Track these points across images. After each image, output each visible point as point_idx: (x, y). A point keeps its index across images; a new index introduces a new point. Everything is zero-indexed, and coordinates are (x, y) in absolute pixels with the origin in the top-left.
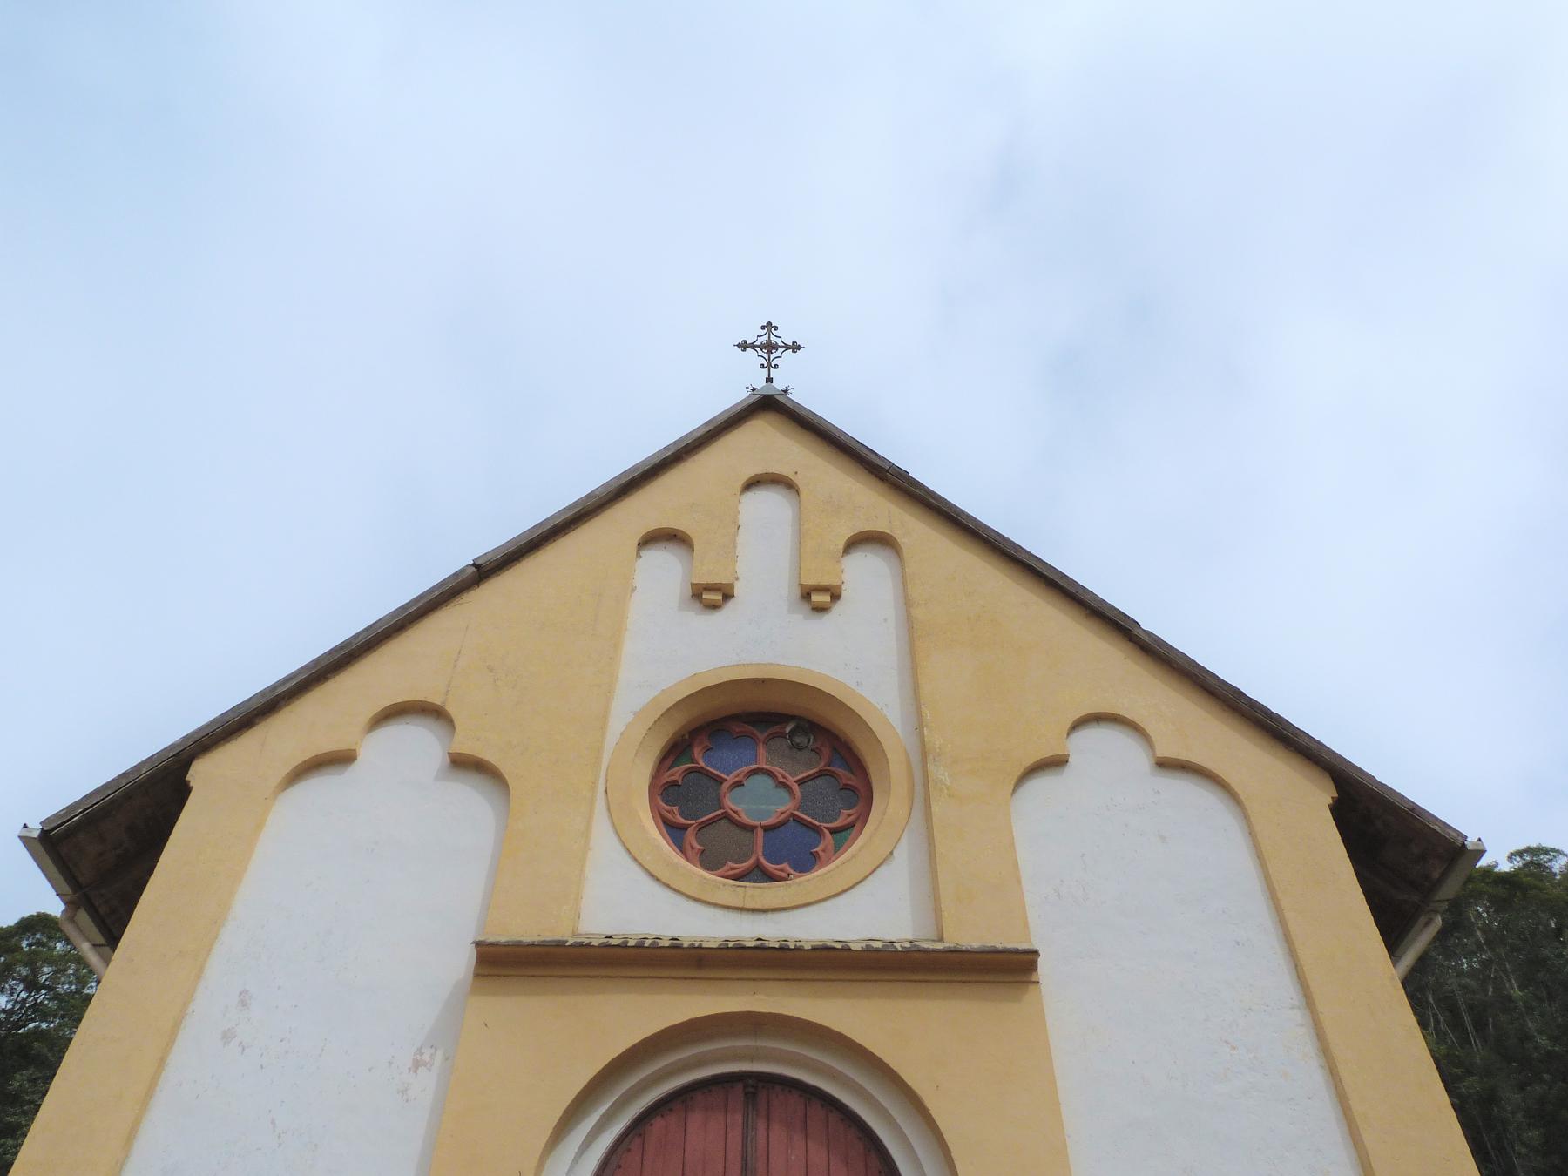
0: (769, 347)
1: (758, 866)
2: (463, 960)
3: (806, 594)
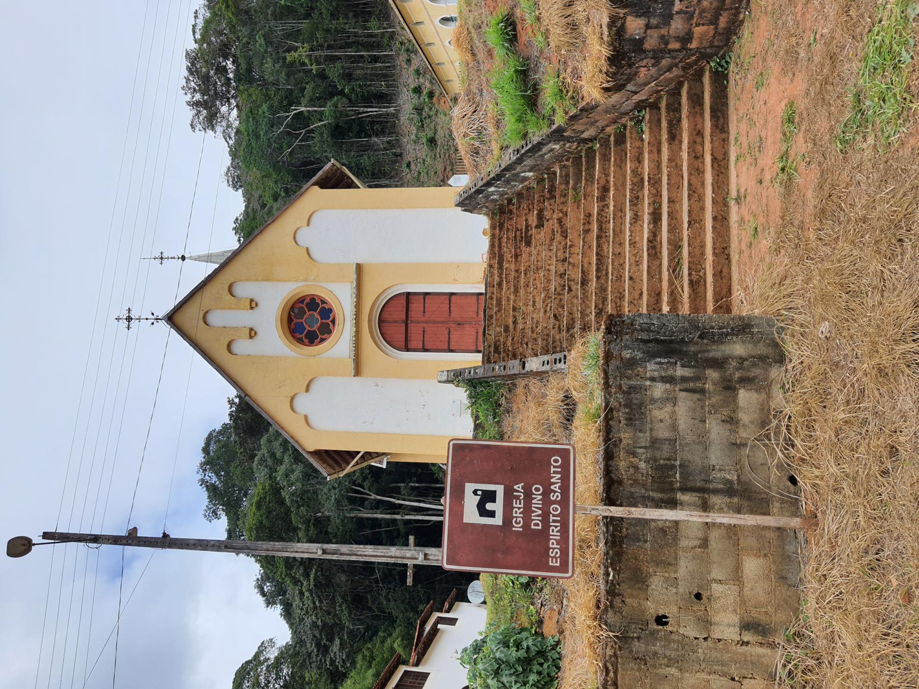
0: (129, 319)
1: (331, 321)
3: (252, 308)
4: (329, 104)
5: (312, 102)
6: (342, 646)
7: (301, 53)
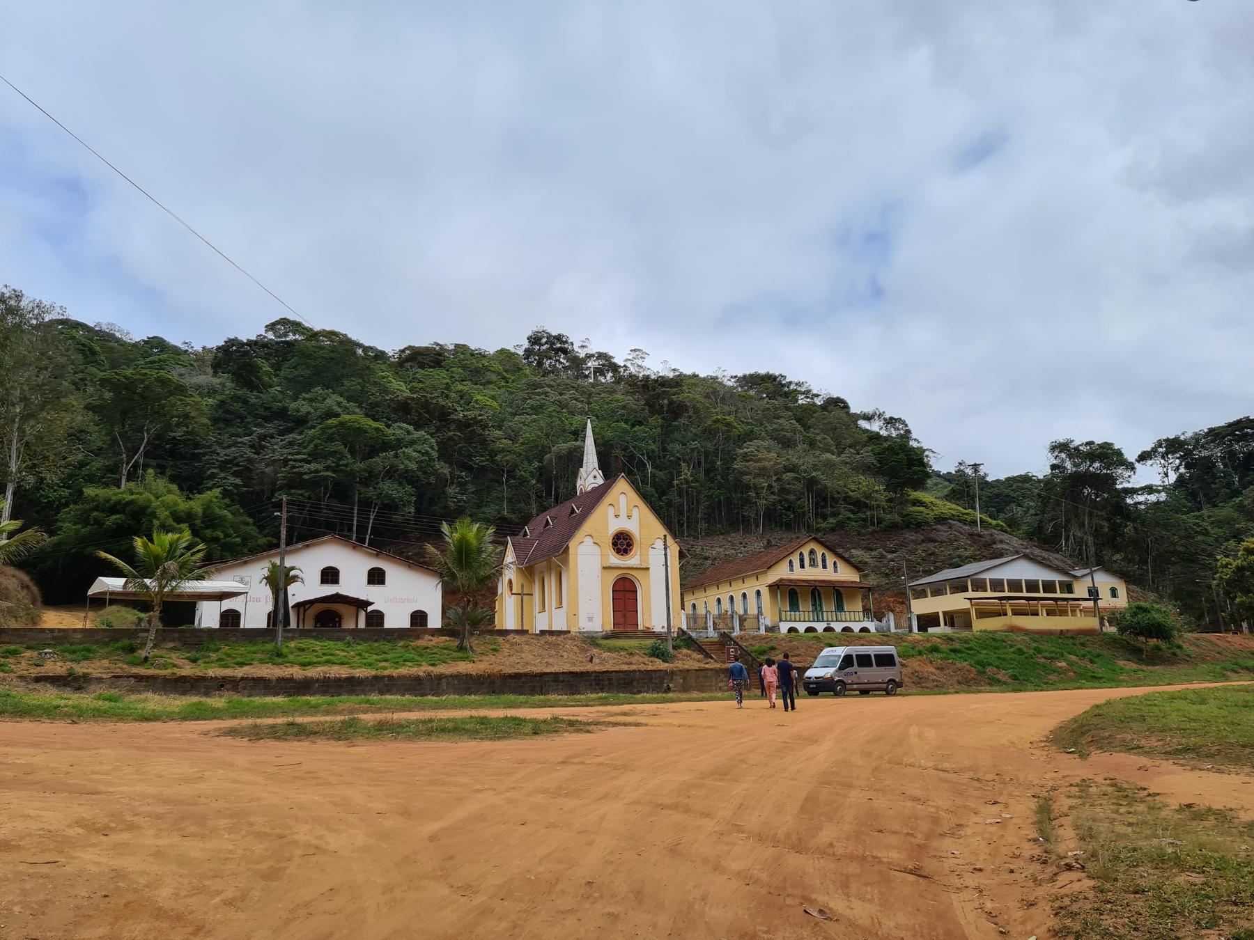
2: (599, 567)
4: (653, 490)
5: (653, 475)
6: (236, 486)
7: (686, 473)
